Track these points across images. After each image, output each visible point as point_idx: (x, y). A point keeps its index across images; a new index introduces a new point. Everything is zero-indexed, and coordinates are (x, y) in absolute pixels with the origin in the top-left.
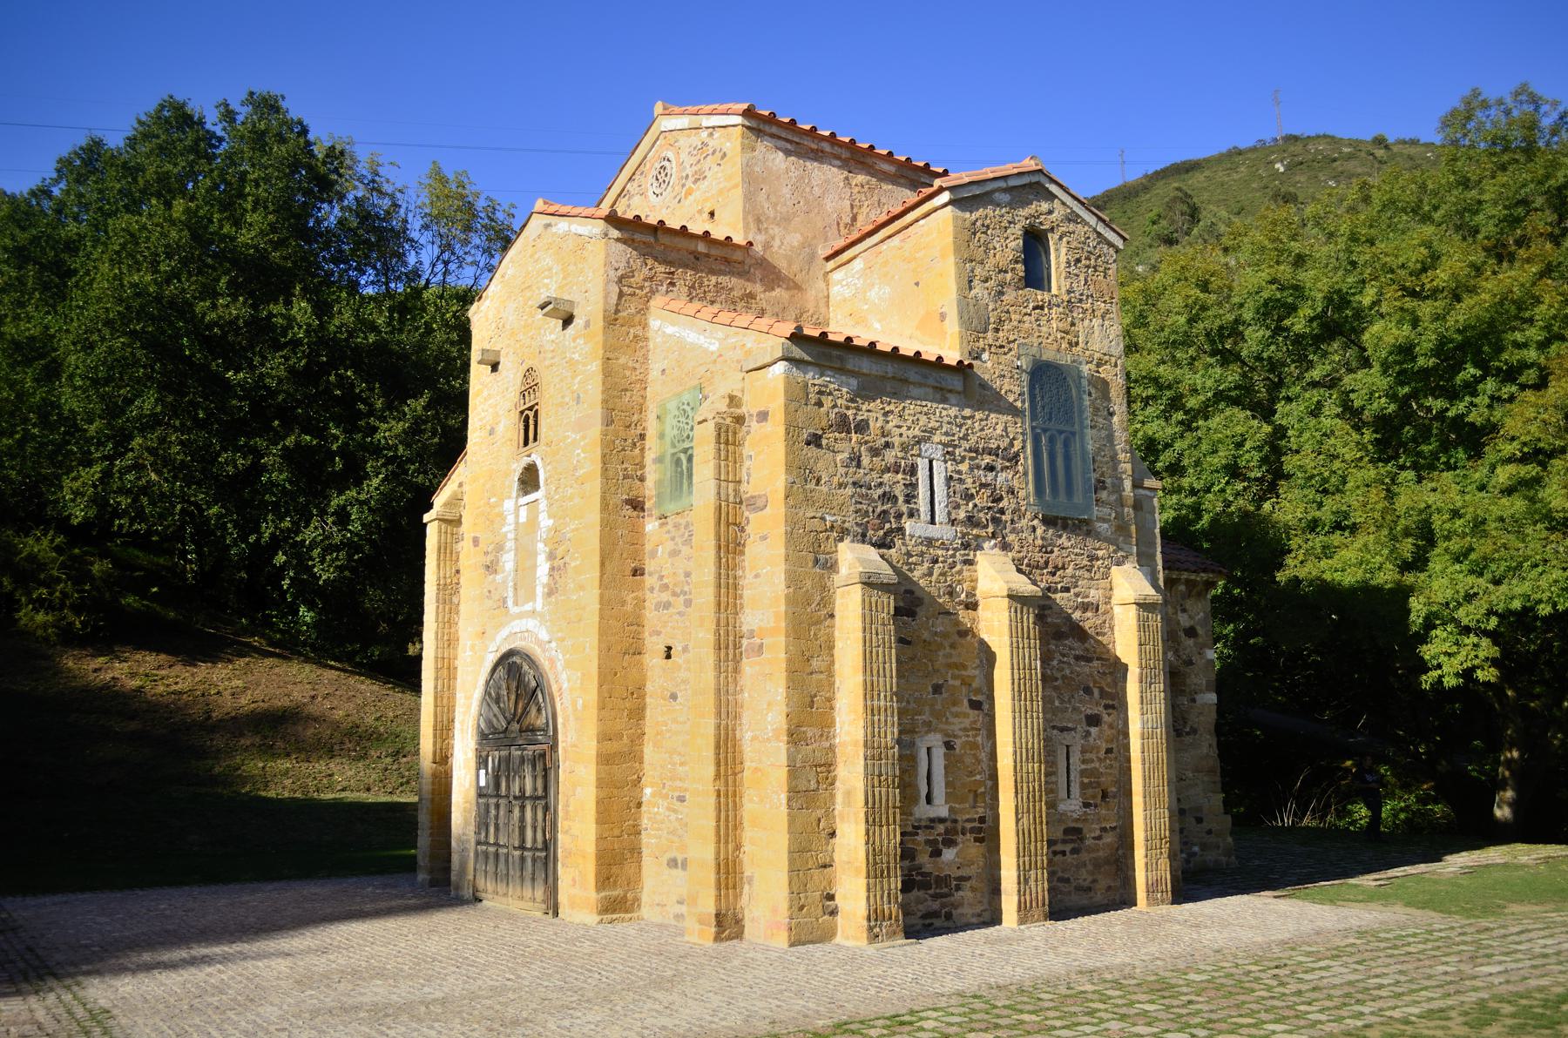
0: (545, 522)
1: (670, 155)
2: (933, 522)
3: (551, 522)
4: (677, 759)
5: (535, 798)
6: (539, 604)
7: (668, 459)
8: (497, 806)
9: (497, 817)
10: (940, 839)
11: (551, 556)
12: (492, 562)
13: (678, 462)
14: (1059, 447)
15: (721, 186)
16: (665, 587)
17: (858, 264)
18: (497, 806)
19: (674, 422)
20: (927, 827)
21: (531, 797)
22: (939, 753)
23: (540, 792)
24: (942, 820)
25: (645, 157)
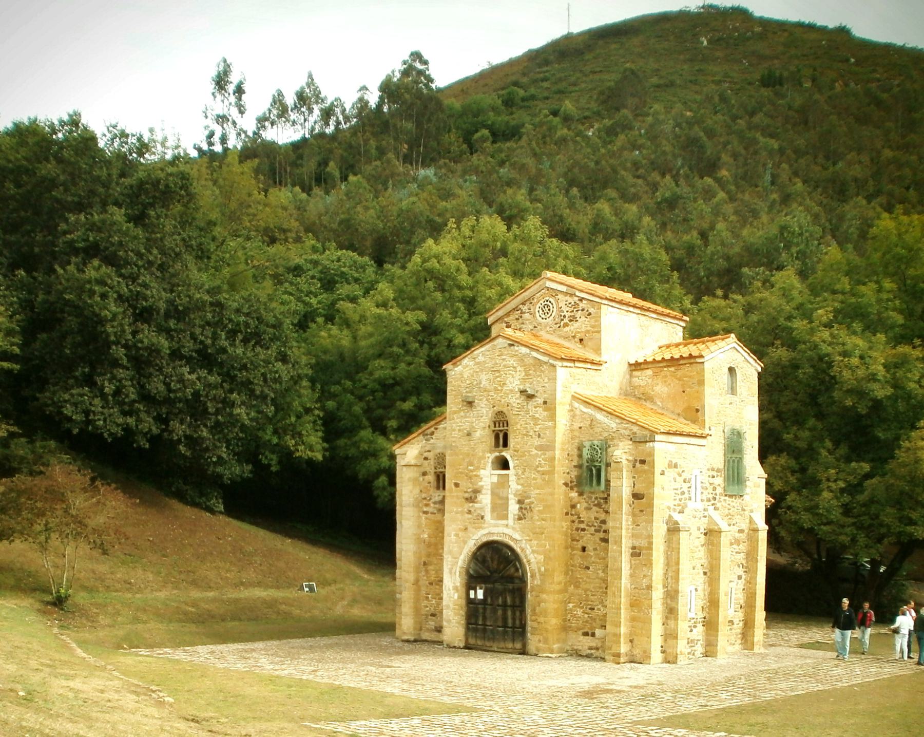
0: (514, 486)
1: (552, 301)
3: (520, 487)
4: (590, 593)
5: (513, 606)
6: (511, 522)
7: (585, 467)
8: (485, 609)
9: (484, 613)
11: (520, 502)
13: (591, 471)
15: (589, 328)
16: (582, 522)
17: (649, 372)
18: (485, 609)
21: (510, 606)
23: (518, 603)
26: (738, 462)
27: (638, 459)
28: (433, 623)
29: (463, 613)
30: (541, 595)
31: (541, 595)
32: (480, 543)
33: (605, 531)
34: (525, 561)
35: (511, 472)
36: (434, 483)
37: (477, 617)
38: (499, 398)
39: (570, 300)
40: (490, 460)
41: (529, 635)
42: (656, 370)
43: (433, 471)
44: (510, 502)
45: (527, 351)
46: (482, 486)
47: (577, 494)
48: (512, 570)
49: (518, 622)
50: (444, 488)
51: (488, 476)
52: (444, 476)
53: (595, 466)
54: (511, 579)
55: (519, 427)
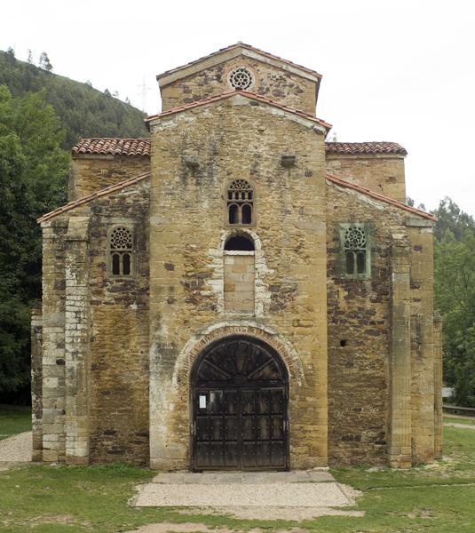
1: (247, 69)
3: (272, 271)
8: (224, 422)
9: (223, 425)
11: (271, 288)
12: (193, 283)
16: (343, 313)
17: (337, 164)
18: (224, 422)
19: (348, 235)
25: (225, 62)
27: (413, 244)
28: (110, 443)
29: (189, 428)
30: (308, 398)
31: (308, 398)
32: (213, 340)
33: (373, 323)
34: (284, 358)
35: (258, 252)
36: (110, 267)
37: (211, 433)
38: (237, 164)
39: (274, 73)
40: (224, 238)
41: (291, 447)
42: (346, 163)
43: (108, 249)
44: (257, 289)
45: (281, 113)
46: (212, 270)
47: (333, 282)
48: (267, 370)
49: (277, 434)
50: (127, 271)
51: (216, 256)
52: (127, 258)
53: (355, 251)
54: (265, 381)
55: (270, 200)
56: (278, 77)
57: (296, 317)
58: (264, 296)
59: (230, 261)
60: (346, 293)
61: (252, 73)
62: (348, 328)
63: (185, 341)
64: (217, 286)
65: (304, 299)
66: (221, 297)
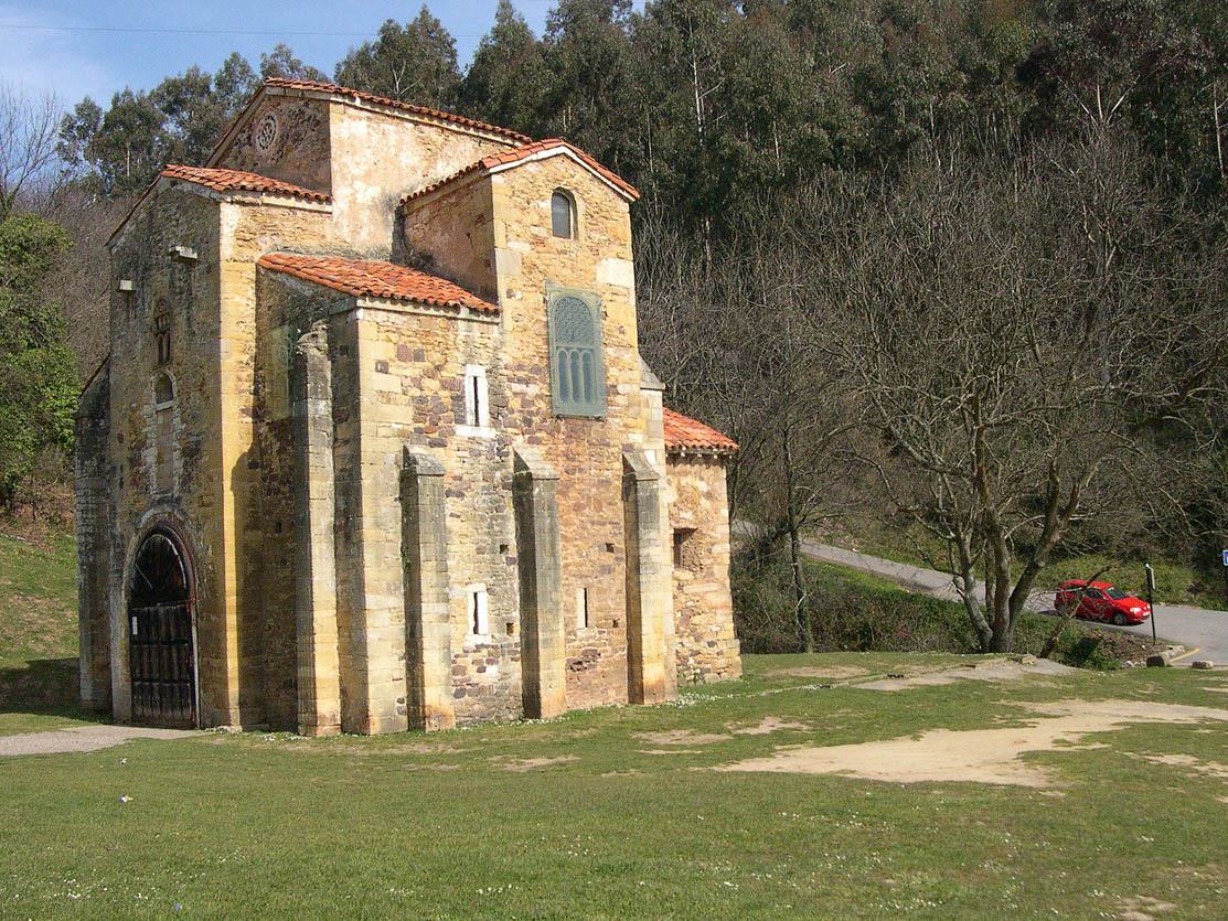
1: (273, 114)
2: (477, 424)
10: (485, 659)
14: (581, 363)
16: (274, 478)
17: (425, 214)
20: (475, 651)
21: (175, 642)
22: (483, 598)
24: (487, 647)
25: (254, 113)
26: (586, 357)
39: (293, 107)
56: (297, 112)
57: (202, 491)
58: (178, 464)
59: (161, 420)
60: (278, 444)
61: (275, 118)
62: (280, 501)
63: (129, 539)
64: (150, 456)
65: (205, 462)
66: (154, 470)
